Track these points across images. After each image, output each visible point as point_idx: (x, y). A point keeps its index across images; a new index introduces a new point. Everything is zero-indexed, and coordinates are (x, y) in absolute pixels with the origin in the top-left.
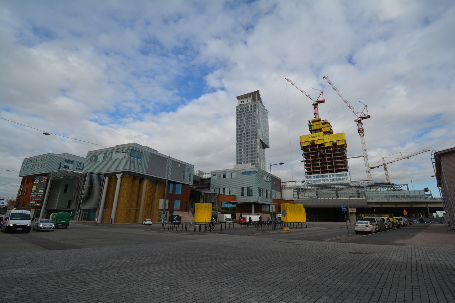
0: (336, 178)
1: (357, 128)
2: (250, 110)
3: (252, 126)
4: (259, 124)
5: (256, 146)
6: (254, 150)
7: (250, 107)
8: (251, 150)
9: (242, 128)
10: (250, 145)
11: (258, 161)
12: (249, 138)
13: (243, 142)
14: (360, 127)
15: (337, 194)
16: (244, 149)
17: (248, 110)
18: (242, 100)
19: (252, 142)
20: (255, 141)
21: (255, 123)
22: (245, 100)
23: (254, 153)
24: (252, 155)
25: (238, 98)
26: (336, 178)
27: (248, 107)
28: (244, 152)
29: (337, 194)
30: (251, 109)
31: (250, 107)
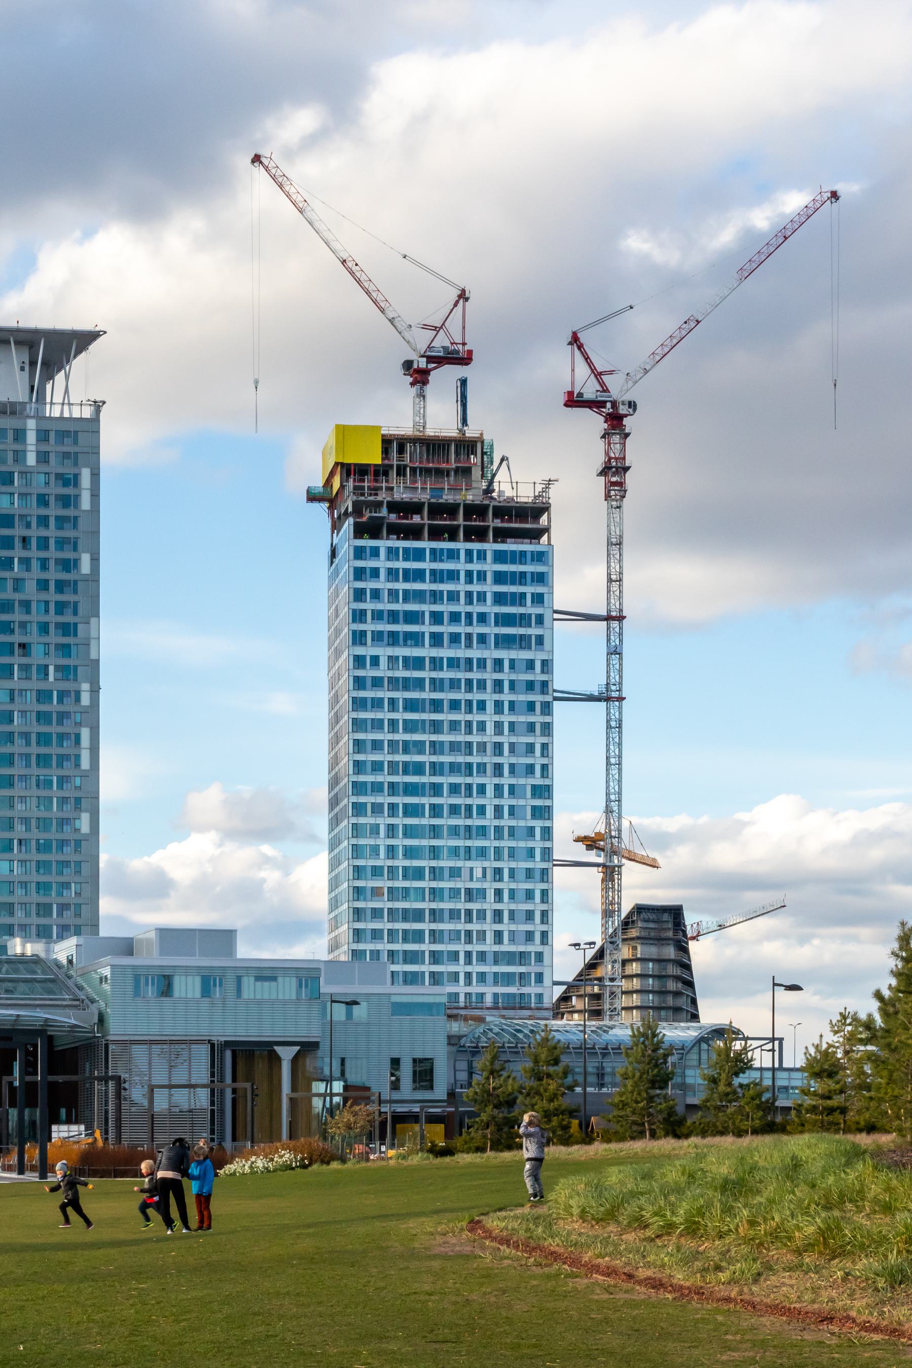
0: (496, 969)
1: (599, 461)
2: (31, 459)
3: (43, 585)
4: (94, 577)
5: (68, 727)
6: (54, 750)
7: (31, 437)
8: (34, 750)
12: (25, 668)
14: (616, 450)
17: (20, 456)
20: (62, 695)
21: (69, 565)
26: (496, 969)
27: (19, 435)
30: (43, 457)
31: (31, 437)
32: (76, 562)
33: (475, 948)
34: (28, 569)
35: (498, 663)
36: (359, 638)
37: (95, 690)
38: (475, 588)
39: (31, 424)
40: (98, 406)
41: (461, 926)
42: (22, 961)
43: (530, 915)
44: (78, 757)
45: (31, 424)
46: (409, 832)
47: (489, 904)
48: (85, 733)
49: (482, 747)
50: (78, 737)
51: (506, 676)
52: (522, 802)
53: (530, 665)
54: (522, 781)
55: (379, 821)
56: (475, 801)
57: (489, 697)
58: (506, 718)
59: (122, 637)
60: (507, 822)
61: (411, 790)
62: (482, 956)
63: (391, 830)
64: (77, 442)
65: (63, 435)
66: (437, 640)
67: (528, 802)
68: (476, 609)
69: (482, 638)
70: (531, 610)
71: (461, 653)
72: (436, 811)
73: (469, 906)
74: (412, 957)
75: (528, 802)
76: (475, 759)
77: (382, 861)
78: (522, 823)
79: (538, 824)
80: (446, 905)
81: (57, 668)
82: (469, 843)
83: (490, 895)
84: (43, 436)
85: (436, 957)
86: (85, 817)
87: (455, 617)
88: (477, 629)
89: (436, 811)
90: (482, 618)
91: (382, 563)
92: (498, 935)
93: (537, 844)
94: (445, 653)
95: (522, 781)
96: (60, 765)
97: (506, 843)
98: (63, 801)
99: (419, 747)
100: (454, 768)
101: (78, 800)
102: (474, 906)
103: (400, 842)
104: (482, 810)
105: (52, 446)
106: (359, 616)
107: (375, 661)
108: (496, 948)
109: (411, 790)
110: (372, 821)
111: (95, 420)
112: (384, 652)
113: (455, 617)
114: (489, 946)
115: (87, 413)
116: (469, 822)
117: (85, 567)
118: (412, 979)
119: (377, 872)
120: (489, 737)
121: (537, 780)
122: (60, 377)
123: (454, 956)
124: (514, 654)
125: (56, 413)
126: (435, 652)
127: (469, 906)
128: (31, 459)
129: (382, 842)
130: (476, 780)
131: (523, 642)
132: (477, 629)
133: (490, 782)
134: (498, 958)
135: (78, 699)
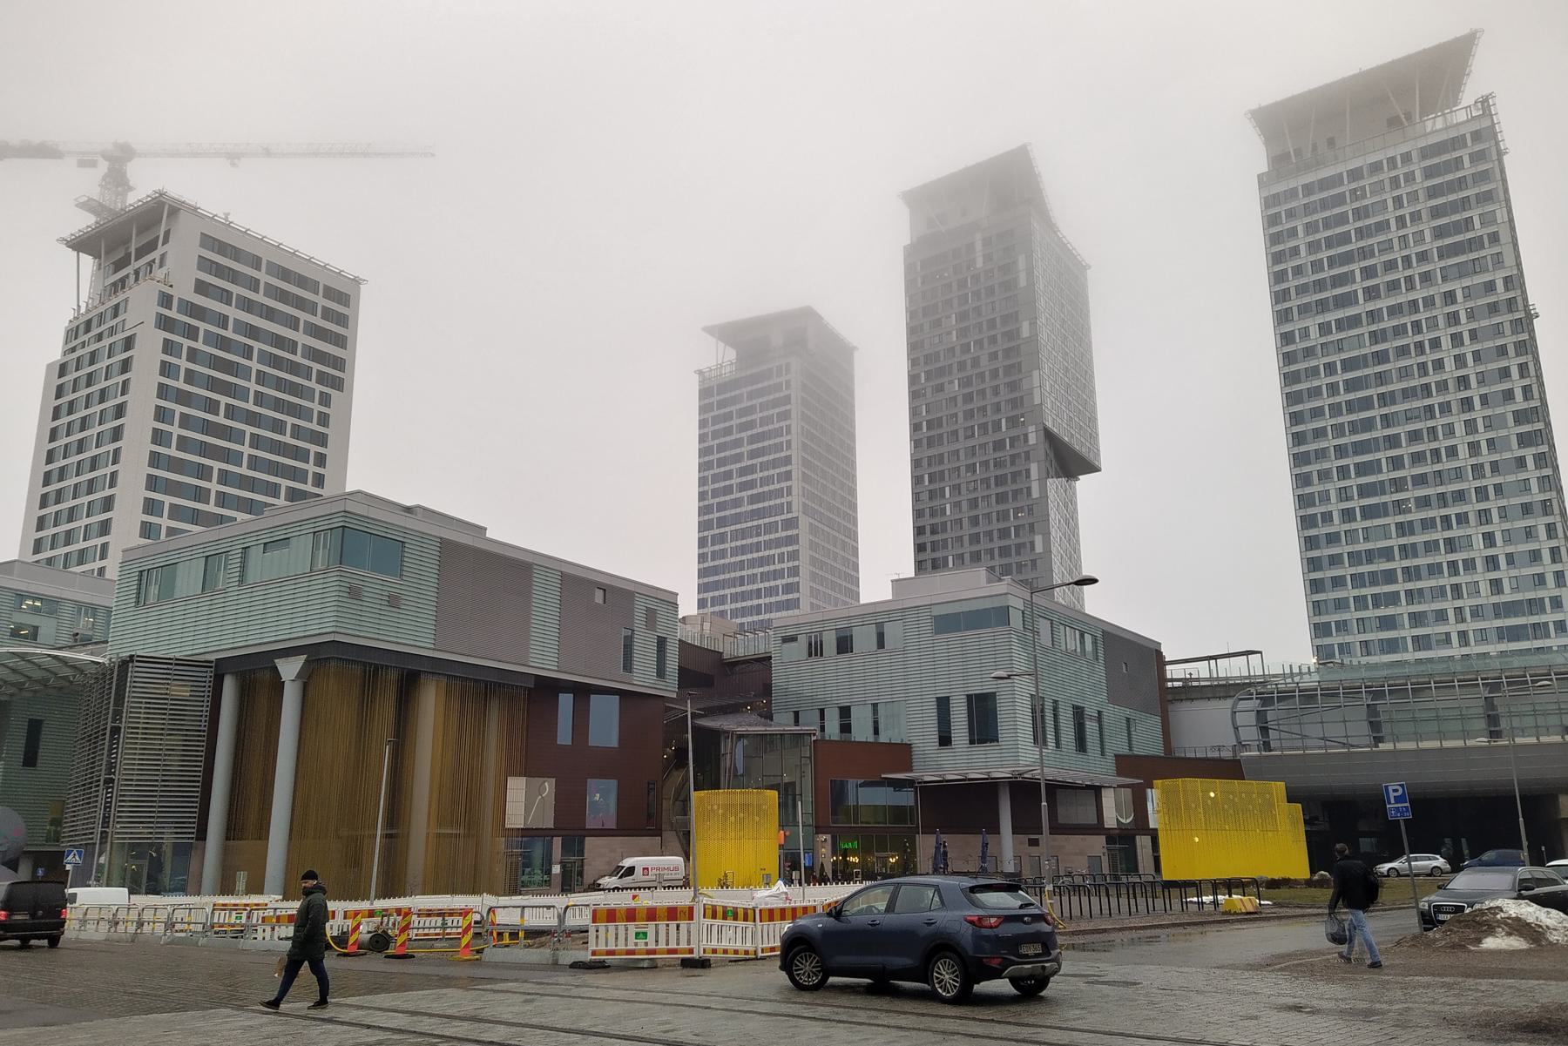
0: (1499, 623)
6: (1009, 488)
8: (994, 490)
9: (941, 372)
10: (985, 464)
11: (1039, 548)
13: (946, 449)
15: (1493, 720)
19: (999, 446)
23: (1010, 506)
24: (1003, 516)
28: (957, 505)
29: (1493, 720)
32: (1018, 330)
33: (1467, 603)
34: (981, 348)
41: (1446, 581)
43: (1535, 556)
44: (1029, 489)
46: (1364, 491)
49: (1443, 386)
50: (1028, 471)
52: (1503, 433)
53: (1490, 287)
54: (1499, 410)
55: (1329, 486)
56: (1443, 444)
61: (1360, 448)
62: (1477, 612)
63: (1344, 495)
66: (1371, 293)
70: (1479, 230)
72: (1396, 463)
73: (1452, 557)
74: (1388, 623)
76: (1435, 400)
78: (1507, 455)
79: (1529, 453)
80: (1422, 561)
81: (1008, 420)
82: (1441, 489)
83: (1479, 542)
85: (1417, 619)
89: (1396, 463)
92: (1496, 585)
94: (1383, 304)
95: (1499, 410)
96: (1015, 498)
97: (1490, 481)
99: (1366, 404)
100: (1409, 417)
101: (1032, 526)
102: (1458, 557)
103: (1356, 503)
104: (1452, 452)
107: (1305, 333)
108: (1496, 599)
109: (1360, 448)
110: (1321, 488)
112: (1312, 323)
114: (1486, 598)
116: (1437, 467)
118: (1392, 646)
119: (1333, 539)
121: (1520, 403)
123: (1441, 616)
126: (1371, 306)
127: (1452, 557)
129: (1335, 507)
134: (1501, 610)
135: (1026, 440)
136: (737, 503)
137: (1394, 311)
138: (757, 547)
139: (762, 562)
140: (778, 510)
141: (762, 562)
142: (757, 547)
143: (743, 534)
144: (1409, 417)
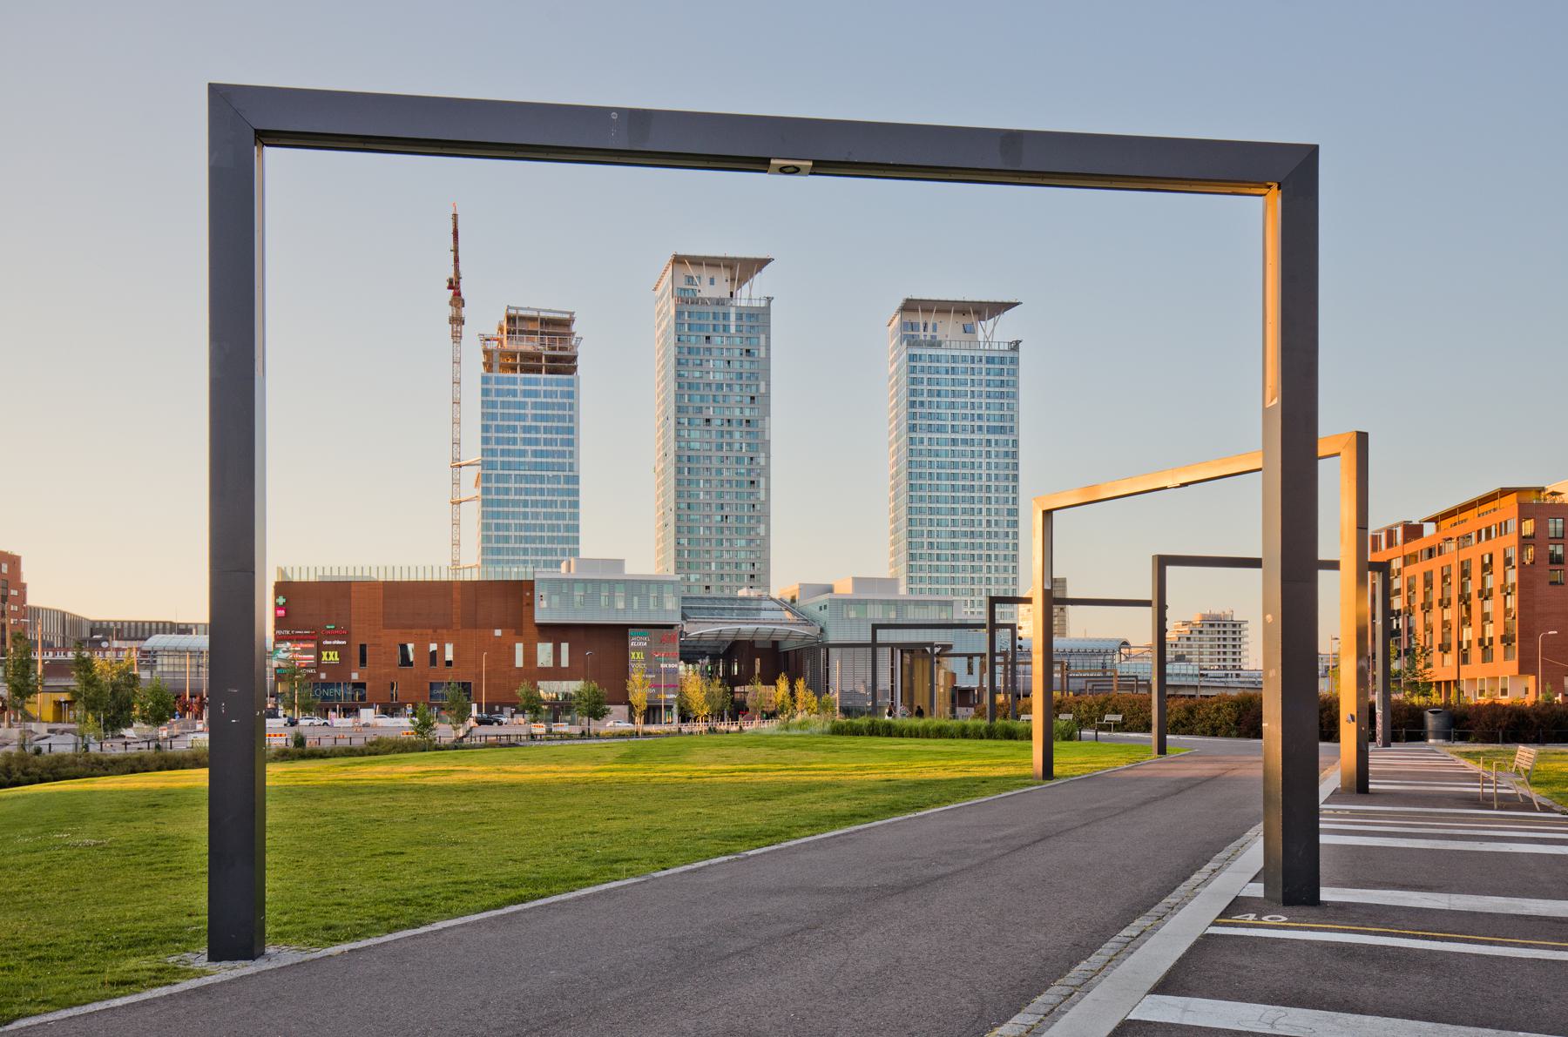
2: (733, 330)
4: (767, 395)
7: (733, 317)
16: (706, 481)
17: (726, 328)
18: (691, 271)
22: (706, 273)
25: (678, 260)
27: (726, 316)
28: (708, 493)
30: (739, 330)
31: (733, 317)
35: (989, 441)
36: (912, 428)
37: (768, 457)
38: (976, 400)
39: (733, 310)
40: (769, 300)
42: (743, 599)
45: (733, 310)
47: (984, 575)
48: (762, 481)
51: (993, 449)
57: (984, 461)
58: (993, 472)
59: (781, 426)
60: (993, 529)
64: (758, 319)
65: (750, 316)
67: (1004, 518)
68: (977, 412)
69: (980, 428)
71: (968, 436)
75: (1004, 518)
77: (925, 551)
79: (1011, 530)
81: (749, 445)
84: (739, 317)
86: (762, 527)
87: (965, 417)
88: (977, 423)
90: (980, 417)
91: (925, 387)
93: (1010, 541)
98: (751, 518)
100: (964, 500)
105: (746, 322)
106: (913, 416)
107: (922, 441)
111: (768, 308)
113: (965, 417)
115: (763, 304)
117: (762, 390)
120: (984, 482)
121: (1011, 506)
122: (746, 287)
124: (997, 437)
125: (744, 303)
128: (733, 330)
129: (926, 540)
130: (977, 506)
131: (1002, 430)
132: (977, 423)
133: (984, 507)
136: (523, 453)
137: (965, 442)
138: (542, 492)
139: (545, 504)
140: (561, 467)
141: (545, 504)
142: (542, 492)
143: (527, 479)
144: (964, 500)
